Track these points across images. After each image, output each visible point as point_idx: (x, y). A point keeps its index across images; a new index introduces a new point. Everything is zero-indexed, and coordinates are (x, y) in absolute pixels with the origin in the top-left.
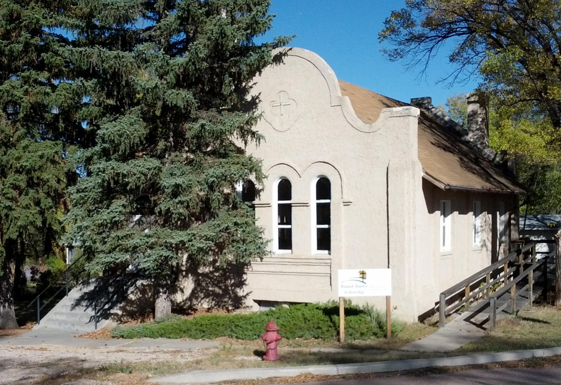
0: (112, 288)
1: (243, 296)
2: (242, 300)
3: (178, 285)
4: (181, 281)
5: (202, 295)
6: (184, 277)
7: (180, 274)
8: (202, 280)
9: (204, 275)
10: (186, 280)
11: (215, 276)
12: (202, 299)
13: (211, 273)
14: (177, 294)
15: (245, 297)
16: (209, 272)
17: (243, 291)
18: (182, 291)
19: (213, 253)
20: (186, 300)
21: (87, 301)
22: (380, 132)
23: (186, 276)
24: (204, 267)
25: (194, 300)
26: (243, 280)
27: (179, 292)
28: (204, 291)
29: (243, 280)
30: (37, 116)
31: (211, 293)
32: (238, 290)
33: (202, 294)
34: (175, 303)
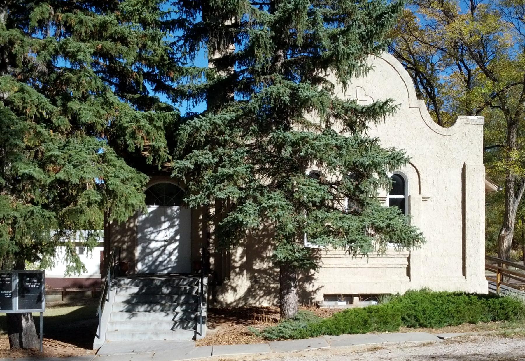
0: (168, 290)
1: (312, 291)
2: (311, 295)
3: (229, 284)
4: (233, 279)
5: (261, 293)
6: (237, 274)
7: (232, 271)
8: (259, 276)
9: (260, 271)
10: (239, 277)
11: (276, 272)
12: (261, 297)
13: (270, 268)
14: (227, 294)
15: (315, 292)
16: (267, 268)
17: (313, 286)
18: (234, 290)
19: (273, 247)
20: (240, 299)
21: (146, 305)
22: (457, 136)
23: (241, 273)
24: (262, 263)
25: (250, 299)
26: (310, 274)
27: (230, 291)
28: (264, 288)
29: (310, 274)
30: (55, 93)
31: (273, 290)
32: (307, 285)
33: (262, 292)
34: (225, 303)
